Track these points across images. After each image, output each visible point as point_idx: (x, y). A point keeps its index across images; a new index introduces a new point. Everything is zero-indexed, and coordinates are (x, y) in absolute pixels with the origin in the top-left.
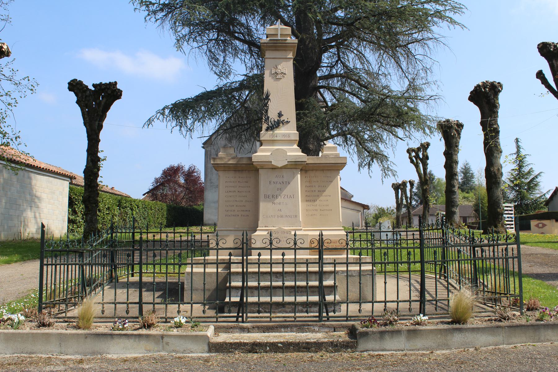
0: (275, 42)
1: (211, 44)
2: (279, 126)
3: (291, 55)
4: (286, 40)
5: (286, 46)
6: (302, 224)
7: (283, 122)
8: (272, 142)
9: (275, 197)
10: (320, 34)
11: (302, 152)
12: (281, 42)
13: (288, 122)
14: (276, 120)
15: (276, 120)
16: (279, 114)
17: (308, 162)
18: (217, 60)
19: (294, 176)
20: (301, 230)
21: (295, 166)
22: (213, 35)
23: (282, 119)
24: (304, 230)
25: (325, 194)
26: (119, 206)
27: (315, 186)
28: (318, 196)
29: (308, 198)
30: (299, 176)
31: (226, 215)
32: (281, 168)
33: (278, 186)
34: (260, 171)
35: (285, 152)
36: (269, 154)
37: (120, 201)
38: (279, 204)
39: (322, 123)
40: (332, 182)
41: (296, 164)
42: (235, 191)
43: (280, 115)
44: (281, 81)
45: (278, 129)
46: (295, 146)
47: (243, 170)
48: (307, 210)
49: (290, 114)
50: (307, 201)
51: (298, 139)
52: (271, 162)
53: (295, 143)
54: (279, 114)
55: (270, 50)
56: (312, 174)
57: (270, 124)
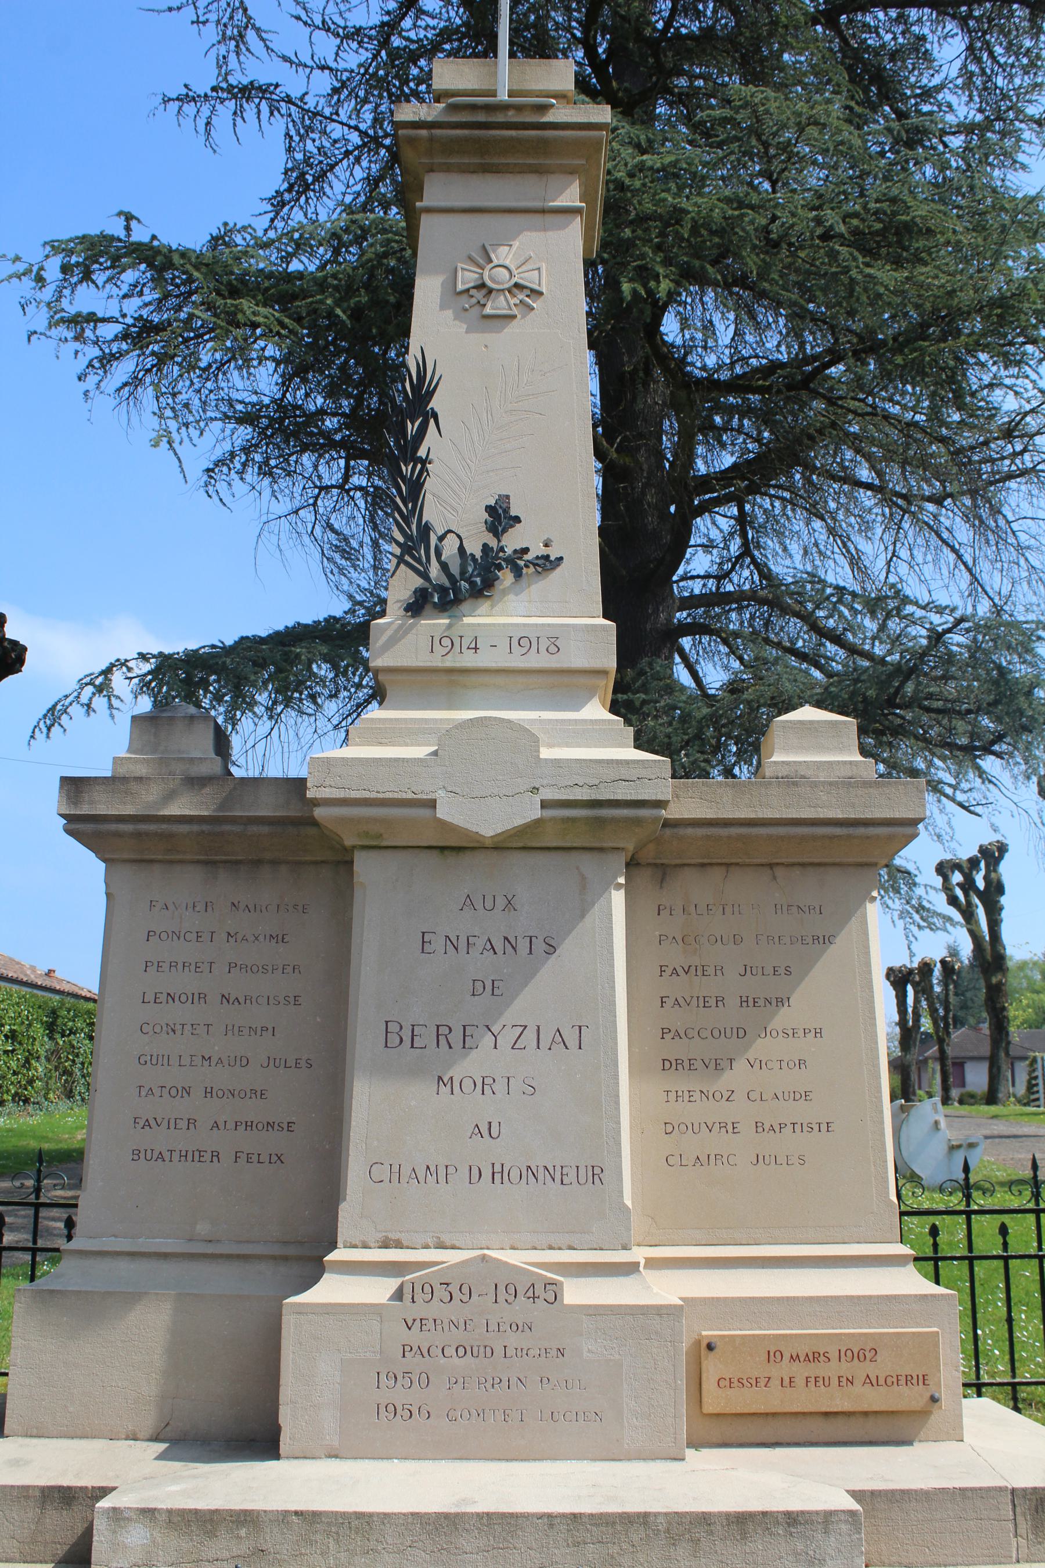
0: (481, 117)
1: (325, 503)
3: (571, 196)
4: (543, 108)
5: (543, 147)
6: (637, 1225)
7: (517, 563)
8: (446, 682)
9: (455, 1038)
10: (685, 453)
11: (638, 746)
12: (512, 116)
13: (547, 564)
14: (474, 548)
15: (474, 548)
16: (490, 509)
17: (671, 813)
20: (630, 1269)
21: (586, 830)
22: (332, 472)
23: (512, 541)
24: (653, 1263)
25: (783, 1018)
26: (51, 1028)
27: (719, 970)
28: (741, 1033)
29: (677, 1049)
30: (618, 899)
31: (136, 1154)
32: (504, 846)
34: (364, 866)
35: (526, 739)
36: (420, 752)
37: (54, 1013)
38: (484, 1085)
39: (698, 736)
40: (827, 940)
41: (600, 823)
42: (202, 997)
43: (500, 518)
44: (512, 329)
45: (484, 606)
46: (596, 711)
47: (258, 863)
48: (669, 1128)
50: (669, 1065)
51: (611, 662)
52: (432, 804)
53: (590, 693)
54: (490, 509)
55: (447, 169)
56: (697, 888)
57: (434, 570)
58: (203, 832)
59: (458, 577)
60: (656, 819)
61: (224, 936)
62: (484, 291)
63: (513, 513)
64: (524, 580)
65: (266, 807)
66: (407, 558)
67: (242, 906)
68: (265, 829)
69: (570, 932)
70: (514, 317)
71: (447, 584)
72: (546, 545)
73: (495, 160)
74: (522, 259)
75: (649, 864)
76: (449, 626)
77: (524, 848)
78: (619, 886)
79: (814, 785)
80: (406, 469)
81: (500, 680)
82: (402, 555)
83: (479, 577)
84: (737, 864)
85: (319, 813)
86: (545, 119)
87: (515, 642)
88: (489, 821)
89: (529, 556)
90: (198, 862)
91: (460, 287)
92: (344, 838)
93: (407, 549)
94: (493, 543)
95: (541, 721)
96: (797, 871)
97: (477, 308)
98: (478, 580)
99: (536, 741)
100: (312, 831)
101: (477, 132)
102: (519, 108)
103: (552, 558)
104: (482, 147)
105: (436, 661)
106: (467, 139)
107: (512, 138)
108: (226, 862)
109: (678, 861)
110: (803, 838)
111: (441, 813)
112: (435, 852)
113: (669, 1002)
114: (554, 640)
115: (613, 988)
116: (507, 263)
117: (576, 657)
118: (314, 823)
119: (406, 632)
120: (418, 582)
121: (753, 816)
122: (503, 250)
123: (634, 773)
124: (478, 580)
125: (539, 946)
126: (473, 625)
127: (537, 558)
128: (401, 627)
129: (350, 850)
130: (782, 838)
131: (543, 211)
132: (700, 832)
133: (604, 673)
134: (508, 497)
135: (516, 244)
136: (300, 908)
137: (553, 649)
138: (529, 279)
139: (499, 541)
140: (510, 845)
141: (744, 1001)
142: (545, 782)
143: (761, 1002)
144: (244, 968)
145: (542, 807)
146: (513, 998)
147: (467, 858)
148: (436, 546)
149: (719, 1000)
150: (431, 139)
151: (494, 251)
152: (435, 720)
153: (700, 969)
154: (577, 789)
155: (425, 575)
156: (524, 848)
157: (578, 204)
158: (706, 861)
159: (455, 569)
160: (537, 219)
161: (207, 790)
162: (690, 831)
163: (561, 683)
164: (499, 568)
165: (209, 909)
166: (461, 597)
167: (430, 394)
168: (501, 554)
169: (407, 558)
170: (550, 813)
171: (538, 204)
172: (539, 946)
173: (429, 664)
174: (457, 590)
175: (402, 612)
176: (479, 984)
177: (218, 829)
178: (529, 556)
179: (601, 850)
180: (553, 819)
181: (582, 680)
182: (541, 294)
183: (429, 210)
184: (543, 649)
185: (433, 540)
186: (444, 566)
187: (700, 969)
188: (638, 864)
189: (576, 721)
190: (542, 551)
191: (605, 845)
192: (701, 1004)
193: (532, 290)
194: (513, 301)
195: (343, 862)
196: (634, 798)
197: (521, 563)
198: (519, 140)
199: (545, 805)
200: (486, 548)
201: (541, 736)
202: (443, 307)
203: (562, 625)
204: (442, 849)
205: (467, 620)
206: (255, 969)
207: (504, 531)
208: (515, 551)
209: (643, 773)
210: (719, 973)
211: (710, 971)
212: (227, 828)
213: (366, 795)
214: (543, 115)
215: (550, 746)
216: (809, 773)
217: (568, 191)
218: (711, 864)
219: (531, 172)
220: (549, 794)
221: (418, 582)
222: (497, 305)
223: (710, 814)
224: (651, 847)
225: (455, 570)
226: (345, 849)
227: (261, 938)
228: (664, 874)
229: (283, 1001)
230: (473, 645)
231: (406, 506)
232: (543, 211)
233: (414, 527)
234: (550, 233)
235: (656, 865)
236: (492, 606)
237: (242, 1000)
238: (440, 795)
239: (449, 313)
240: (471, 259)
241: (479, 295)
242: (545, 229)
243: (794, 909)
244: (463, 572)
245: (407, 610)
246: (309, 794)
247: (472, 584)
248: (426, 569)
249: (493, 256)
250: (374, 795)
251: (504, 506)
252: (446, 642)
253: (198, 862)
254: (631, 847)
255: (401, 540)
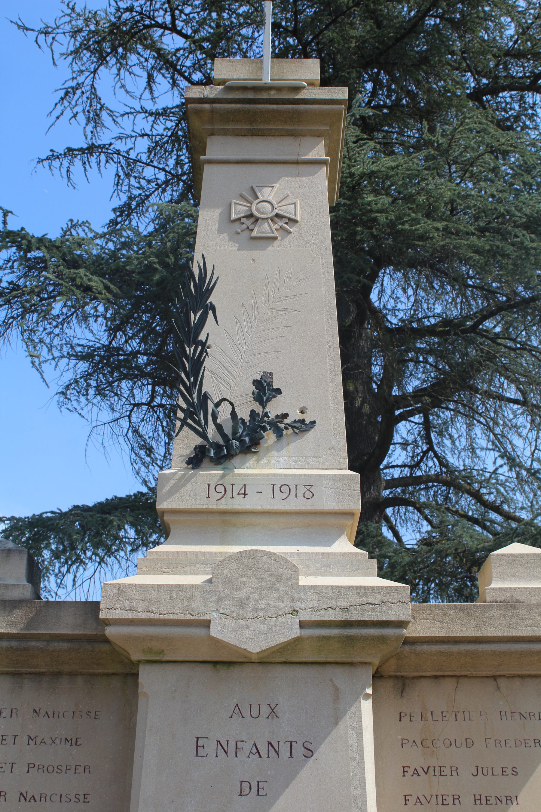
0: (250, 95)
2: (256, 442)
3: (319, 151)
4: (297, 89)
7: (279, 426)
8: (220, 521)
12: (273, 95)
13: (303, 427)
14: (244, 414)
15: (244, 414)
16: (257, 383)
18: (150, 451)
19: (338, 709)
21: (340, 648)
22: (142, 395)
23: (274, 408)
27: (454, 770)
30: (366, 707)
33: (246, 767)
34: (148, 677)
36: (198, 580)
41: (350, 640)
43: (264, 390)
44: (274, 247)
45: (252, 460)
46: (344, 545)
47: (58, 674)
49: (315, 387)
51: (357, 506)
52: (207, 624)
53: (340, 531)
54: (257, 383)
55: (225, 133)
56: (433, 698)
57: (211, 431)
58: (11, 647)
59: (230, 437)
60: (398, 637)
61: (26, 739)
62: (252, 220)
63: (275, 386)
64: (284, 440)
65: (66, 626)
66: (189, 421)
67: (42, 712)
68: (65, 646)
69: (326, 737)
70: (275, 238)
71: (221, 442)
72: (302, 412)
73: (262, 127)
74: (282, 196)
75: (390, 677)
76: (223, 476)
77: (285, 663)
78: (367, 696)
79: (529, 607)
80: (189, 350)
81: (265, 520)
82: (185, 418)
83: (248, 437)
84: (466, 676)
85: (109, 631)
86: (298, 97)
87: (277, 489)
88: (256, 639)
89: (288, 421)
90: (7, 673)
91: (233, 217)
92: (131, 653)
93: (189, 414)
94: (259, 409)
95: (299, 554)
96: (517, 682)
97: (247, 232)
98: (247, 439)
99: (296, 570)
100: (104, 647)
101: (247, 106)
102: (279, 89)
103: (307, 422)
104: (252, 117)
105: (212, 504)
106: (239, 111)
107: (273, 111)
108: (30, 673)
109: (415, 674)
110: (522, 654)
111: (215, 632)
112: (209, 667)
113: (412, 800)
114: (309, 487)
115: (364, 788)
116: (270, 199)
117: (328, 502)
118: (106, 640)
119: (188, 481)
120: (199, 441)
121: (479, 634)
122: (267, 190)
123: (378, 598)
124: (247, 439)
125: (299, 750)
126: (243, 475)
127: (295, 421)
128: (183, 476)
129: (136, 664)
130: (505, 653)
131: (297, 163)
132: (435, 648)
133: (351, 514)
134: (271, 374)
135: (277, 186)
136: (92, 715)
137: (308, 495)
138: (288, 211)
139: (264, 408)
140: (273, 660)
141: (477, 799)
142: (303, 606)
143: (492, 800)
144: (42, 768)
145: (301, 627)
146: (276, 798)
147: (236, 671)
148: (213, 411)
149: (456, 798)
150: (212, 111)
151: (260, 191)
152: (210, 554)
153: (437, 769)
154: (331, 612)
155: (203, 435)
156: (285, 663)
157: (324, 157)
158: (439, 673)
159: (228, 430)
160: (293, 168)
161: (16, 612)
162: (425, 647)
163: (315, 523)
164: (264, 429)
165: (14, 715)
166: (233, 452)
167: (209, 291)
168: (266, 419)
169: (189, 421)
170: (308, 632)
171: (293, 157)
172: (299, 750)
173: (206, 507)
174: (229, 447)
175: (184, 465)
176: (246, 785)
177: (24, 645)
178: (288, 421)
179: (351, 664)
180: (310, 638)
181: (333, 520)
182: (296, 221)
183: (210, 162)
184: (300, 495)
185: (211, 406)
186: (219, 428)
187: (437, 769)
188: (382, 676)
189: (328, 554)
190: (299, 416)
191: (355, 660)
192: (440, 802)
193: (290, 219)
194: (274, 227)
195: (130, 674)
196: (380, 618)
197: (282, 426)
198: (278, 112)
199: (303, 625)
200: (253, 413)
201: (300, 566)
202: (220, 231)
203: (316, 475)
204: (215, 663)
205: (237, 471)
206: (50, 769)
207: (268, 400)
208: (277, 416)
209: (388, 598)
210: (454, 773)
211: (447, 771)
212: (33, 644)
213: (151, 616)
214: (297, 94)
215: (307, 575)
216: (523, 597)
217: (316, 149)
218: (444, 676)
219: (289, 135)
220: (306, 616)
221: (199, 441)
222: (263, 229)
223: (442, 633)
224: (393, 661)
225: (228, 430)
226: (132, 663)
227: (58, 741)
228: (404, 685)
229: (74, 799)
230: (242, 492)
231: (189, 380)
232: (297, 163)
233: (195, 396)
234: (303, 179)
235: (396, 677)
236: (258, 461)
237: (37, 798)
238: (214, 616)
239: (225, 236)
240: (242, 197)
241: (248, 222)
242: (299, 176)
243: (517, 716)
244: (235, 432)
245: (188, 463)
246: (102, 615)
247: (242, 442)
248: (205, 430)
249: (259, 194)
250: (157, 616)
251: (268, 380)
252: (220, 489)
253: (7, 673)
254: (377, 662)
255: (185, 406)
